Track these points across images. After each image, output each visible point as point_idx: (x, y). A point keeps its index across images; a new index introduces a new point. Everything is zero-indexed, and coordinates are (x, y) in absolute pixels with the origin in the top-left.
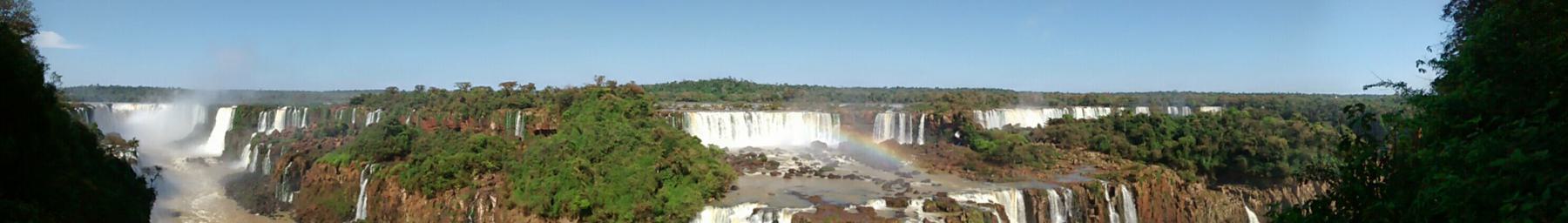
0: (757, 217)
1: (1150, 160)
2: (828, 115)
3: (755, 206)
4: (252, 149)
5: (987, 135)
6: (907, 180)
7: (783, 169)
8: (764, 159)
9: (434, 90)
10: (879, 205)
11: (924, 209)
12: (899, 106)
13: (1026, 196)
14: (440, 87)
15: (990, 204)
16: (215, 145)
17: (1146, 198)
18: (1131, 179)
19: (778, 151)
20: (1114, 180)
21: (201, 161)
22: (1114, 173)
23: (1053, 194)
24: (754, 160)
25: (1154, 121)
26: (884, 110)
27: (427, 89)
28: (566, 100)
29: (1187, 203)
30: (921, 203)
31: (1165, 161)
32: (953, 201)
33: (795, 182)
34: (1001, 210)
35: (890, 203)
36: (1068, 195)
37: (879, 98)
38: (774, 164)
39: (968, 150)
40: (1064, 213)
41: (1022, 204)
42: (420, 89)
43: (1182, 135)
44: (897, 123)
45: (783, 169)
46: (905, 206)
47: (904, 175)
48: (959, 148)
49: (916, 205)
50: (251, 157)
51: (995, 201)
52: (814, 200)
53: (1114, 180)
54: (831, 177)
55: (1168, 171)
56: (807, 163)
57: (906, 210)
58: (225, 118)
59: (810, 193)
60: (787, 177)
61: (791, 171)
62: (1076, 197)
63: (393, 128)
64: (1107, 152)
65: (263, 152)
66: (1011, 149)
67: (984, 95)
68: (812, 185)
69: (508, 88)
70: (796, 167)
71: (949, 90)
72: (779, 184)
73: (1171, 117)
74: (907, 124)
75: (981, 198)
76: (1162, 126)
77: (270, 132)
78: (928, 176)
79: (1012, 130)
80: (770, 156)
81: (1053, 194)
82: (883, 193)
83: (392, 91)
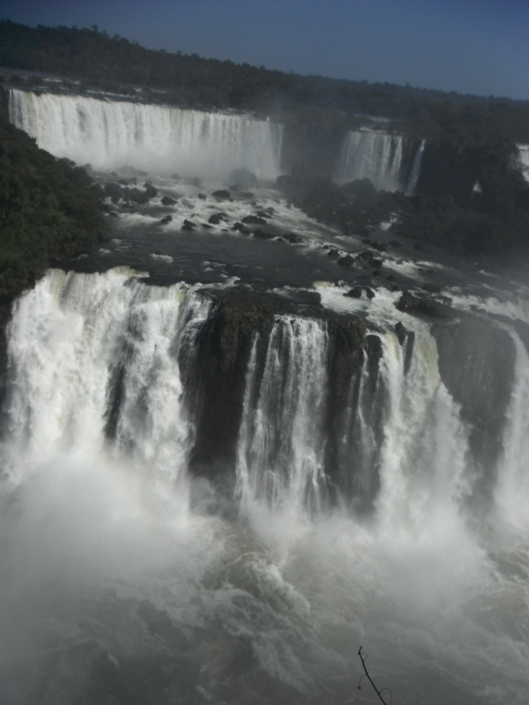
8: (152, 192)
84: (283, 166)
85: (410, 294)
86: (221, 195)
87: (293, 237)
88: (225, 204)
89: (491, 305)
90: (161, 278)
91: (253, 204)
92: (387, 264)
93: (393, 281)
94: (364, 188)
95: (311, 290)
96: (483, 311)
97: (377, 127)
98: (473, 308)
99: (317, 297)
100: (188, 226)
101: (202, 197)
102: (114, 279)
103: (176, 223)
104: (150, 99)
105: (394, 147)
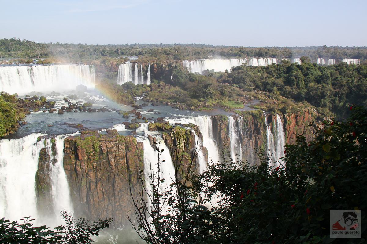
2: (87, 66)
3: (39, 135)
5: (191, 77)
6: (138, 111)
7: (58, 106)
10: (120, 128)
12: (134, 58)
13: (214, 121)
15: (190, 126)
19: (54, 94)
23: (231, 120)
30: (147, 125)
32: (167, 123)
33: (67, 116)
35: (127, 127)
36: (241, 120)
37: (120, 52)
39: (178, 89)
40: (237, 132)
41: (211, 125)
44: (133, 70)
45: (58, 106)
46: (136, 128)
49: (143, 127)
51: (194, 123)
52: (79, 127)
54: (90, 111)
57: (137, 131)
59: (76, 123)
60: (60, 113)
61: (63, 108)
62: (246, 121)
66: (206, 87)
68: (78, 117)
71: (169, 45)
72: (55, 118)
74: (139, 71)
78: (152, 108)
80: (48, 98)
81: (231, 120)
82: (123, 120)
85: (152, 123)
93: (145, 120)
95: (112, 129)
96: (181, 124)
99: (115, 130)
102: (32, 138)
104: (39, 63)
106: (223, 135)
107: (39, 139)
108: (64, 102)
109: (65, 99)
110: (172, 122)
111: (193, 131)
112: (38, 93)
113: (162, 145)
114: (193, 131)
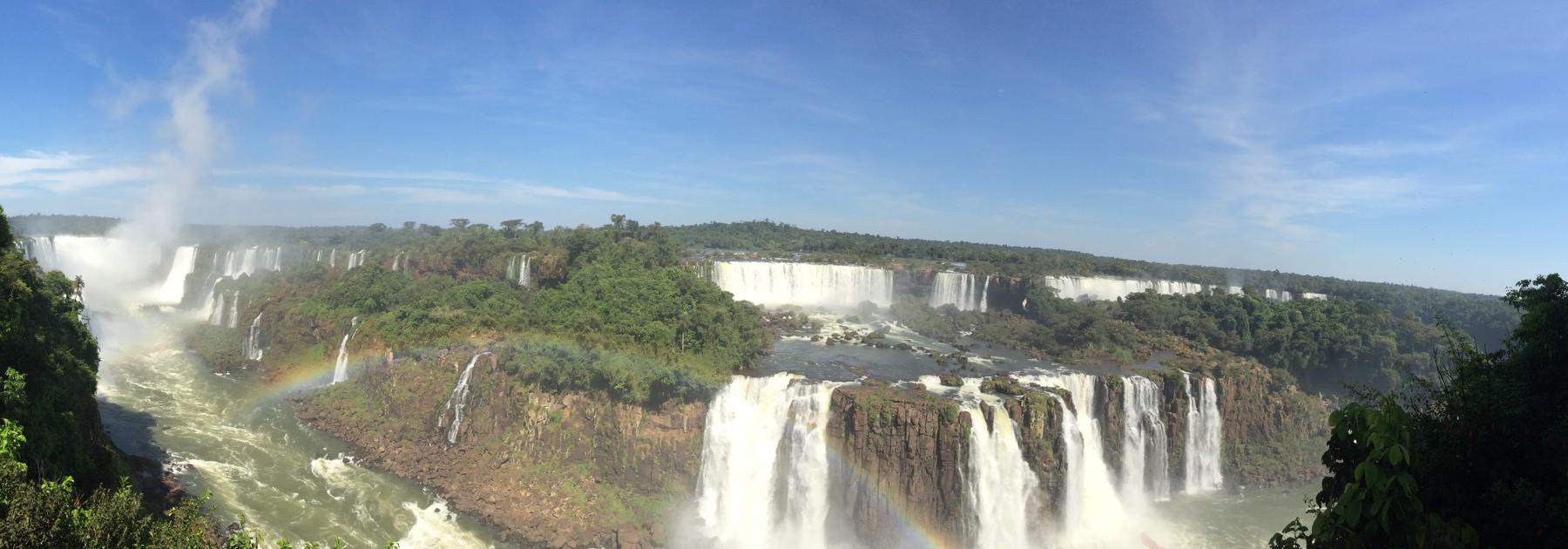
0: (792, 389)
1: (1240, 352)
4: (216, 297)
8: (805, 321)
9: (425, 227)
11: (982, 390)
14: (432, 223)
16: (171, 290)
17: (1231, 396)
18: (1217, 374)
19: (822, 310)
20: (1197, 371)
21: (152, 309)
22: (1199, 362)
24: (788, 321)
25: (1247, 305)
26: (945, 269)
27: (417, 227)
28: (579, 245)
29: (1278, 408)
31: (1255, 353)
32: (1014, 382)
34: (1067, 397)
37: (940, 253)
38: (817, 327)
42: (409, 225)
43: (1279, 326)
44: (959, 286)
45: (826, 333)
47: (961, 348)
48: (1025, 322)
50: (215, 306)
51: (1062, 386)
53: (1197, 371)
54: (880, 346)
55: (1259, 368)
56: (854, 327)
58: (185, 260)
63: (375, 272)
64: (1192, 337)
65: (228, 302)
67: (1059, 259)
69: (510, 229)
70: (839, 332)
73: (1272, 304)
75: (1046, 381)
76: (1257, 313)
77: (236, 277)
79: (1090, 304)
83: (378, 228)
84: (894, 298)
86: (855, 320)
87: (903, 347)
88: (854, 327)
89: (1046, 381)
90: (813, 376)
91: (875, 325)
92: (970, 360)
93: (974, 372)
94: (950, 311)
97: (957, 270)
98: (1032, 385)
99: (924, 387)
100: (830, 342)
101: (839, 321)
102: (782, 379)
103: (824, 341)
104: (802, 261)
105: (969, 282)
106: (1112, 410)
107: (791, 383)
108: (837, 326)
109: (839, 321)
110: (1025, 380)
111: (1061, 401)
112: (799, 308)
113: (1004, 422)
114: (1061, 401)
